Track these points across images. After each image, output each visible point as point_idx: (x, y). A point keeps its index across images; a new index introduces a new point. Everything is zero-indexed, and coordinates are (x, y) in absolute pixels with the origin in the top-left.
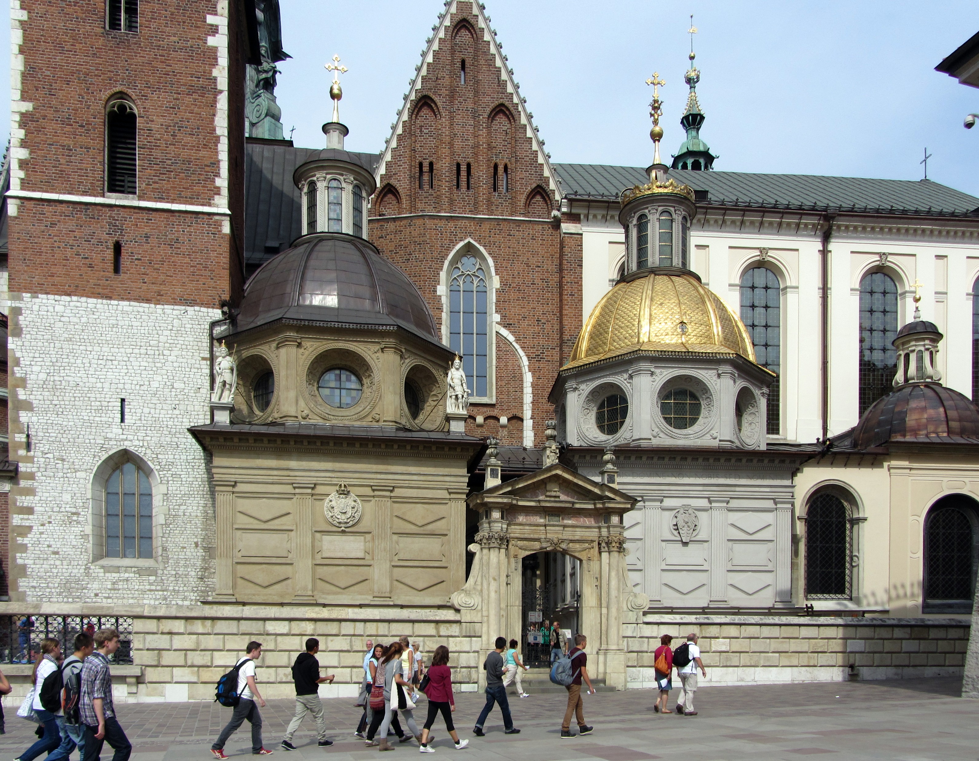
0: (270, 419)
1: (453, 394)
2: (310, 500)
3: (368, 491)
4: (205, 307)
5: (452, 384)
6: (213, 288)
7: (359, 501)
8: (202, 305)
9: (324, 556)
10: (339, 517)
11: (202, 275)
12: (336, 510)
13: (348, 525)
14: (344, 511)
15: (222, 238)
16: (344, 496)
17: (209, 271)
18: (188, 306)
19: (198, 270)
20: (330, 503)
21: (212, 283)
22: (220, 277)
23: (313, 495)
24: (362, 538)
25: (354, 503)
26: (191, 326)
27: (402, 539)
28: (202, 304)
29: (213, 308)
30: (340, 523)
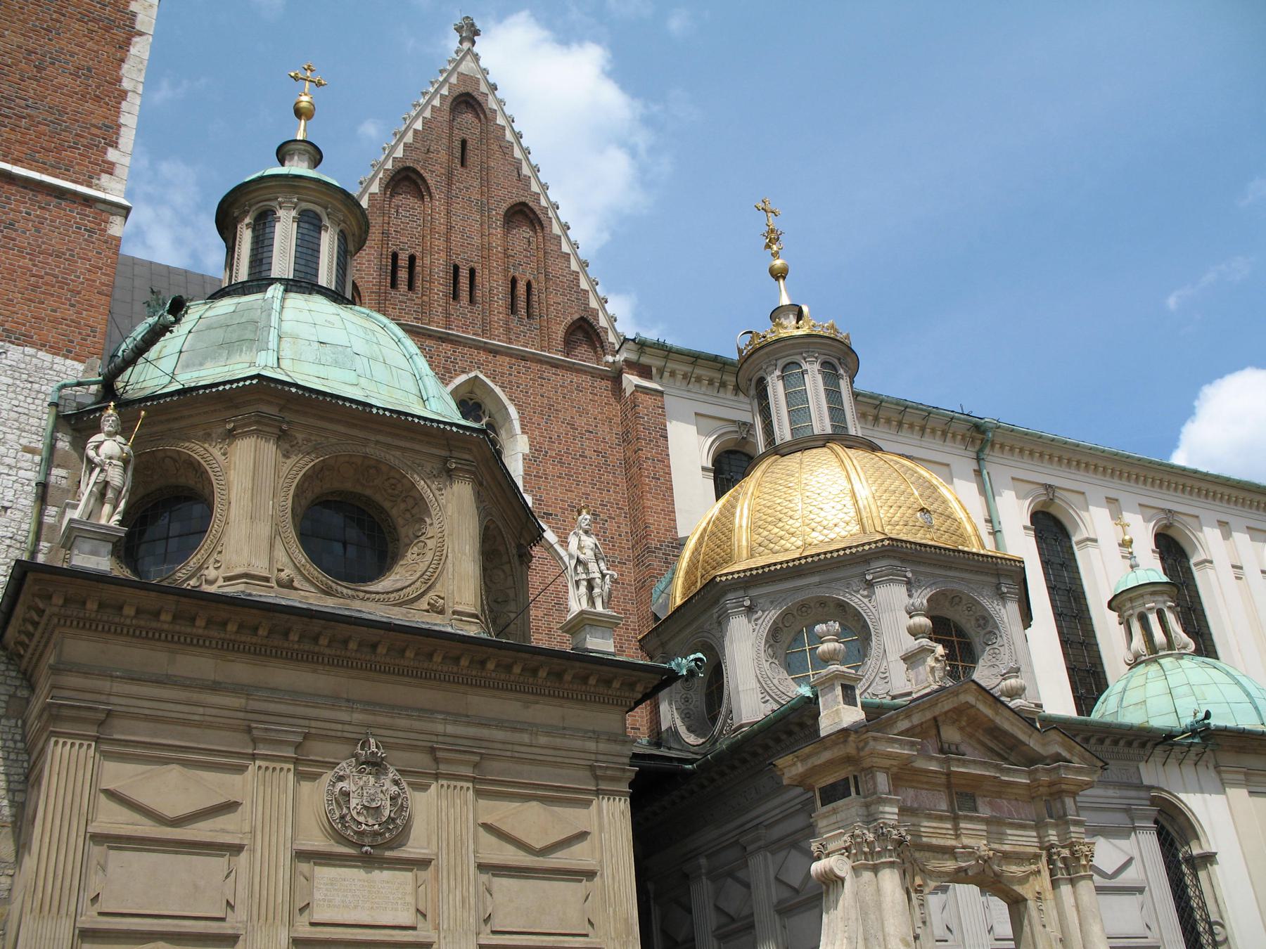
0: (193, 582)
1: (584, 576)
2: (291, 775)
3: (420, 760)
4: (47, 351)
5: (582, 557)
6: (72, 321)
7: (404, 784)
8: (42, 346)
9: (317, 918)
10: (361, 819)
11: (52, 295)
12: (353, 803)
13: (380, 840)
14: (374, 805)
15: (106, 242)
16: (374, 771)
17: (69, 290)
18: (13, 343)
19: (46, 284)
20: (340, 784)
21: (71, 314)
22: (92, 306)
23: (296, 762)
24: (409, 874)
25: (396, 788)
26: (10, 381)
27: (497, 881)
28: (45, 346)
29: (66, 357)
30: (361, 834)
